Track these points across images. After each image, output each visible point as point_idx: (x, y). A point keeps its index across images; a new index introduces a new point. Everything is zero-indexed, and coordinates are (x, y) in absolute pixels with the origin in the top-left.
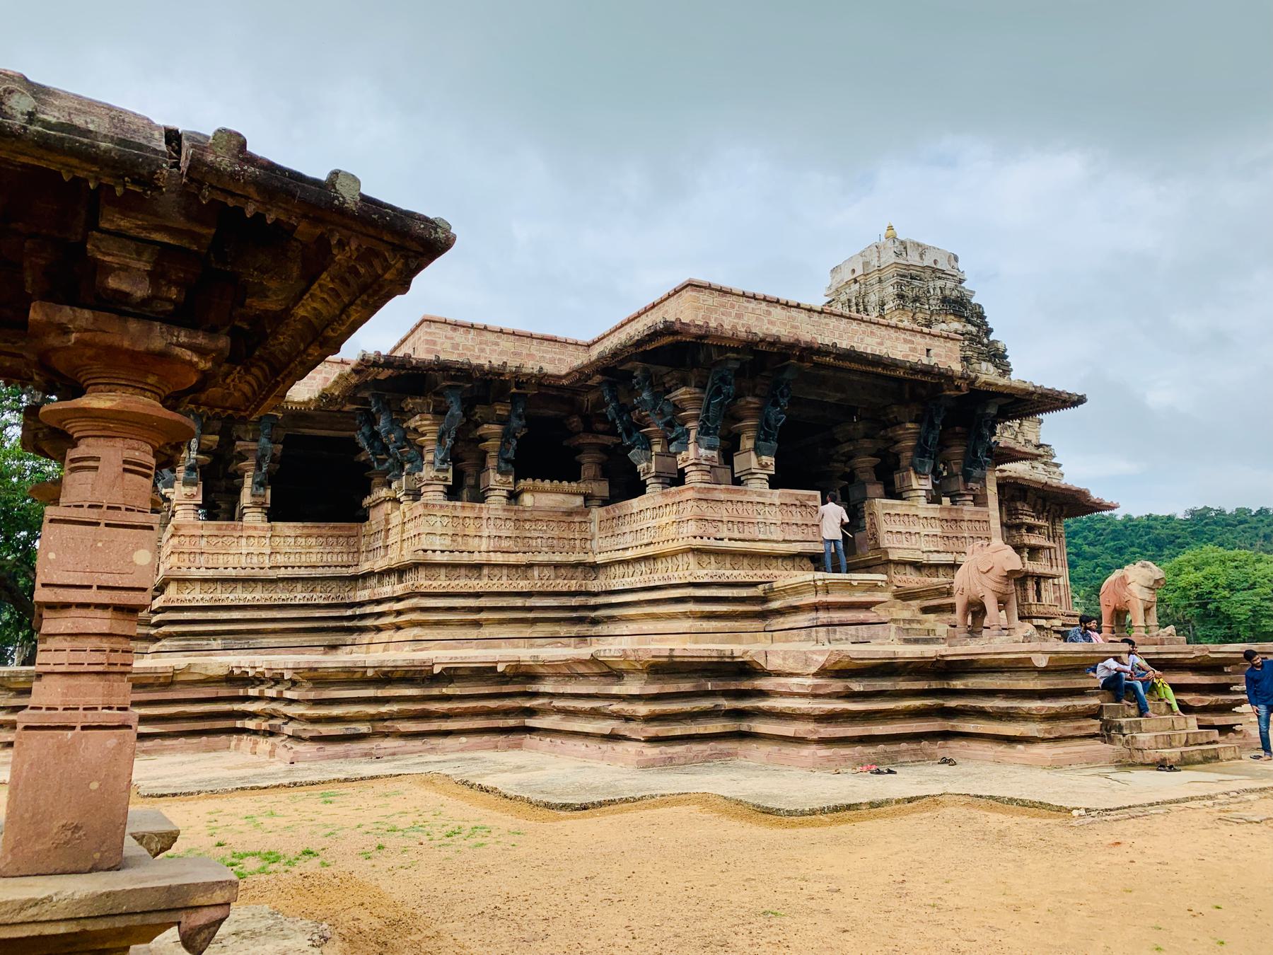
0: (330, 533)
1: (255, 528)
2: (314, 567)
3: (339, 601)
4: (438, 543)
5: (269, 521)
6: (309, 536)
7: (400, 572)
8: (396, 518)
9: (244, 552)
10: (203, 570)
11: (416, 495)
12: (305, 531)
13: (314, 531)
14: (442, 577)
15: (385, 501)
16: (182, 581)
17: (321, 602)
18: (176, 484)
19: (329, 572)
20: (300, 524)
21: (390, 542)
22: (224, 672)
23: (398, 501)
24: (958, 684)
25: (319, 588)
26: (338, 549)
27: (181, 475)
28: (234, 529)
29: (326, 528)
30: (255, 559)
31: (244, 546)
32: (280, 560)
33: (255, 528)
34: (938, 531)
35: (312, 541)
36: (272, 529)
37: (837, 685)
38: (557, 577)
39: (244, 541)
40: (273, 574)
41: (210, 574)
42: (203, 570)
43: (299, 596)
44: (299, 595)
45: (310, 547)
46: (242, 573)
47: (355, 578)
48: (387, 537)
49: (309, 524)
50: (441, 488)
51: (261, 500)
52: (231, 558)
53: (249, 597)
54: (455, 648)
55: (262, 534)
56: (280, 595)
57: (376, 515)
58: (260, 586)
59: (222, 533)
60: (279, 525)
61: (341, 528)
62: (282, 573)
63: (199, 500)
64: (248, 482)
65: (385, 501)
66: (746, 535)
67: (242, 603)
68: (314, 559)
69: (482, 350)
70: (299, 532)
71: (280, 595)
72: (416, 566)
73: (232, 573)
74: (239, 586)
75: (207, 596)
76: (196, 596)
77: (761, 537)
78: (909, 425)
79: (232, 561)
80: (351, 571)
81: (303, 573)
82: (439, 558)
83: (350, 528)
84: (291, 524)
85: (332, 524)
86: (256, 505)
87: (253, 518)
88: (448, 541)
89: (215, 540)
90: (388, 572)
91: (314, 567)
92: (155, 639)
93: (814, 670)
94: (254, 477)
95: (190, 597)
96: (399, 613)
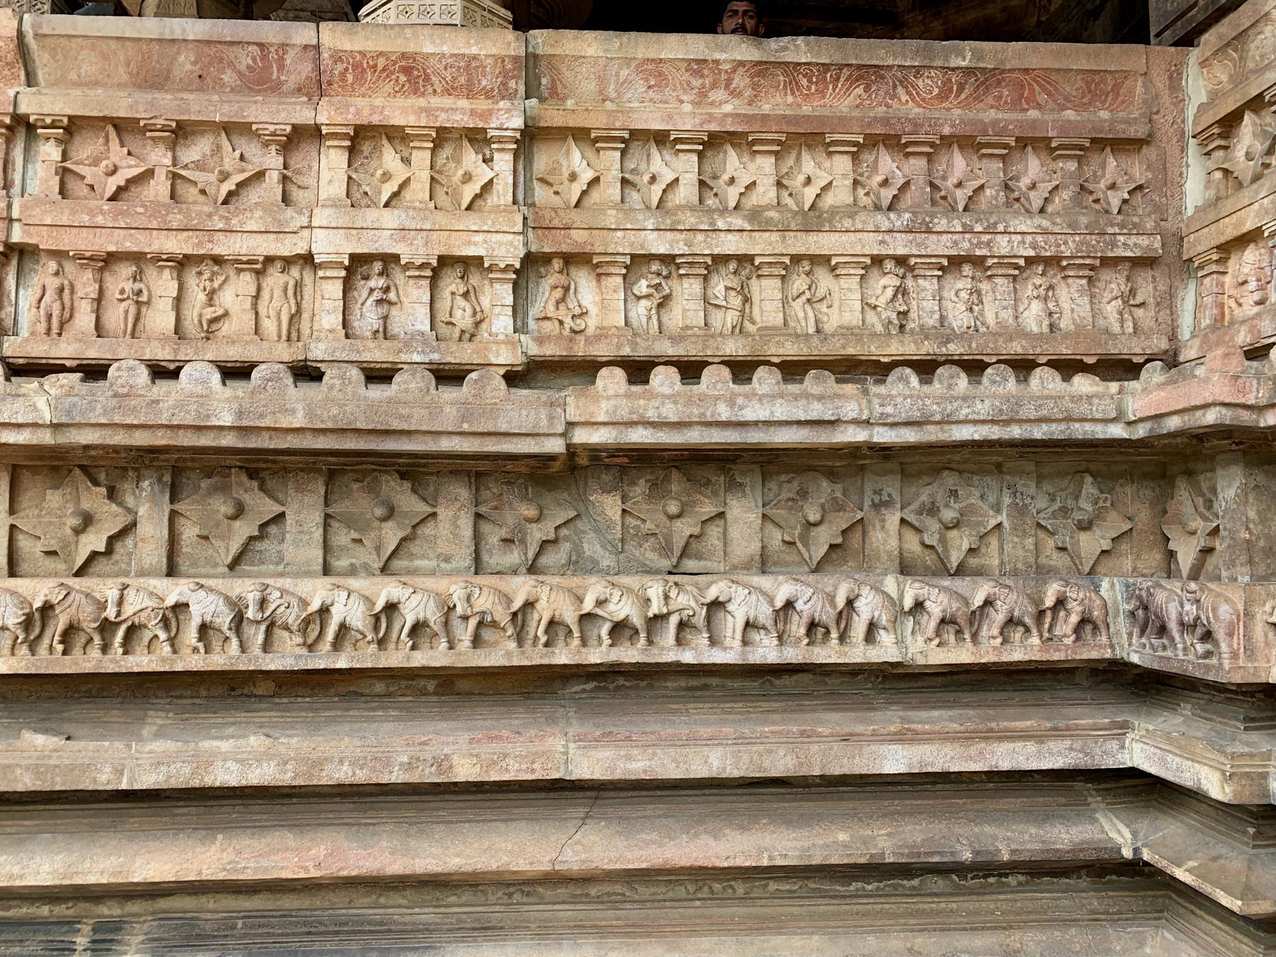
0: (953, 117)
1: (412, 73)
2: (851, 369)
3: (1065, 647)
6: (806, 138)
9: (331, 245)
12: (777, 103)
13: (843, 102)
17: (922, 648)
19: (970, 411)
20: (731, 49)
25: (886, 535)
26: (1016, 237)
28: (260, 81)
30: (413, 308)
32: (599, 309)
33: (412, 73)
35: (825, 174)
39: (330, 167)
46: (294, 412)
49: (799, 49)
53: (349, 611)
55: (458, 112)
56: (600, 592)
59: (164, 106)
60: (586, 52)
61: (1024, 86)
62: (604, 413)
67: (288, 656)
68: (845, 309)
70: (726, 109)
71: (600, 592)
73: (204, 405)
80: (1145, 404)
81: (770, 411)
83: (1097, 87)
85: (965, 54)
91: (851, 369)
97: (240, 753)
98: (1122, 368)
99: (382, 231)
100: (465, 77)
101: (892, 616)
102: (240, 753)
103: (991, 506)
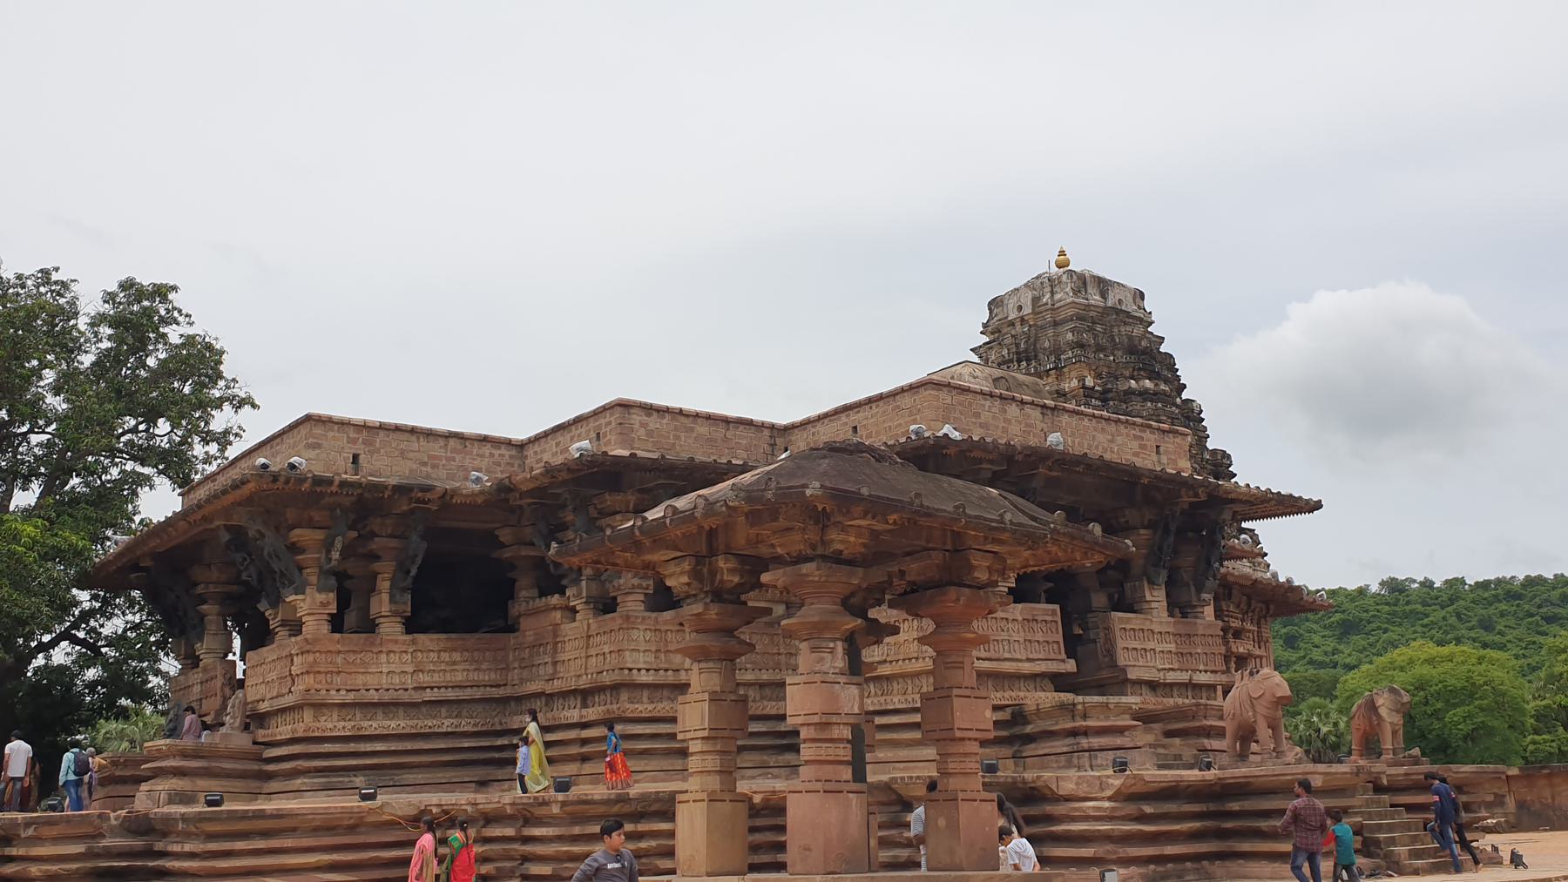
1: (396, 642)
3: (489, 728)
4: (641, 660)
5: (408, 631)
6: (455, 650)
7: (584, 696)
8: (571, 630)
9: (385, 670)
10: (343, 692)
11: (606, 605)
12: (449, 644)
14: (645, 699)
15: (555, 608)
16: (319, 707)
17: (469, 728)
18: (308, 590)
19: (478, 693)
20: (443, 636)
21: (561, 657)
22: (413, 812)
23: (574, 611)
24: (1235, 806)
25: (464, 713)
27: (314, 579)
28: (372, 644)
29: (471, 639)
31: (386, 663)
32: (424, 678)
33: (396, 642)
34: (1172, 647)
35: (456, 656)
36: (414, 642)
37: (1130, 809)
38: (762, 698)
39: (383, 657)
40: (418, 697)
41: (350, 698)
42: (343, 692)
43: (447, 722)
44: (447, 725)
45: (454, 663)
47: (505, 701)
48: (555, 652)
49: (453, 636)
50: (642, 597)
51: (401, 608)
52: (369, 677)
54: (663, 781)
57: (529, 629)
58: (401, 712)
60: (421, 637)
62: (428, 695)
63: (333, 609)
64: (384, 585)
65: (555, 608)
66: (992, 654)
68: (459, 677)
69: (678, 438)
72: (616, 688)
73: (374, 696)
74: (380, 712)
75: (349, 725)
76: (333, 724)
77: (1007, 655)
78: (1142, 531)
79: (371, 680)
81: (451, 694)
82: (644, 678)
84: (435, 636)
86: (395, 614)
87: (391, 628)
88: (651, 658)
89: (351, 657)
90: (565, 694)
92: (270, 776)
93: (1109, 793)
94: (392, 580)
95: (330, 725)
96: (585, 742)
97: (380, 747)
98: (498, 686)
99: (393, 667)
100: (404, 643)
101: (466, 725)
102: (380, 747)
103: (480, 708)
